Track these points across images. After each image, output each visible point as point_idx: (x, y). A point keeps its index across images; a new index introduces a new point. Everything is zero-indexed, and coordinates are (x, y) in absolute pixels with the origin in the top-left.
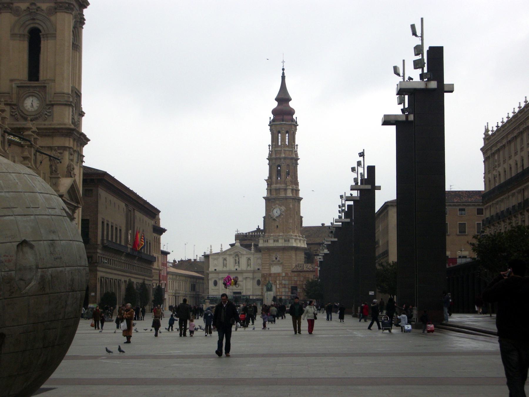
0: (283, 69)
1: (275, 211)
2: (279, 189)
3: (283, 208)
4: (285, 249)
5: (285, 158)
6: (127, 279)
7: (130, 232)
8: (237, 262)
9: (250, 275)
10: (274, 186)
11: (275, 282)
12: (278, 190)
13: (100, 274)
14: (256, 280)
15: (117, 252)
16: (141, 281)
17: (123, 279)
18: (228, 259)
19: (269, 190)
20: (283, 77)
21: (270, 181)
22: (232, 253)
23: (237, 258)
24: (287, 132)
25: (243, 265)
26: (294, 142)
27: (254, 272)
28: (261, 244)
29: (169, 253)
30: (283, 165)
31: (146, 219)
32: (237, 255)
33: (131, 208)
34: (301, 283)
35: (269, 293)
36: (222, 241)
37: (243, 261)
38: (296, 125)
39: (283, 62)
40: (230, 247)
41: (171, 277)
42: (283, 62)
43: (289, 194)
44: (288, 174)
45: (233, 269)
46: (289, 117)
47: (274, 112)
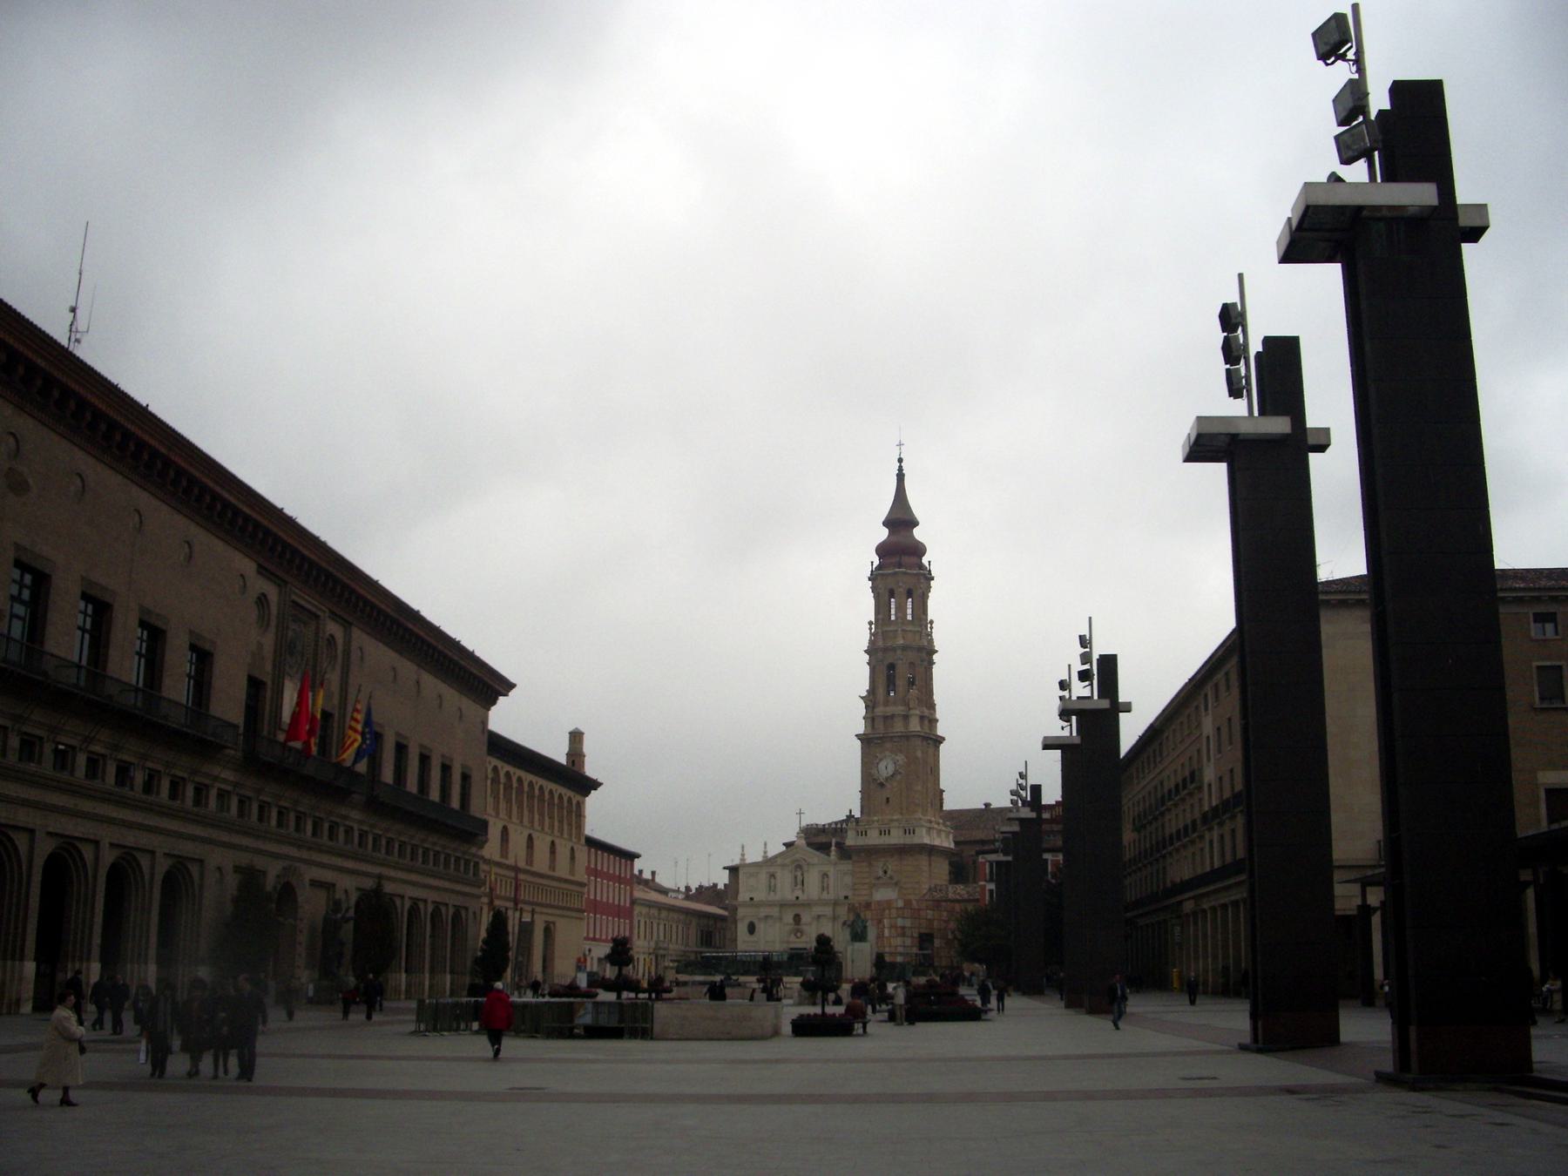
0: (900, 460)
1: (882, 765)
2: (893, 716)
3: (901, 758)
4: (903, 851)
5: (904, 648)
6: (244, 859)
8: (799, 878)
9: (828, 911)
10: (880, 710)
11: (880, 921)
12: (888, 719)
16: (369, 884)
17: (107, 835)
18: (778, 875)
19: (870, 718)
20: (901, 477)
21: (871, 700)
22: (787, 861)
24: (910, 594)
25: (813, 889)
26: (925, 612)
27: (836, 904)
28: (851, 840)
29: (638, 856)
30: (901, 662)
31: (469, 706)
32: (799, 867)
35: (857, 945)
36: (771, 835)
37: (813, 878)
38: (929, 577)
39: (900, 445)
41: (645, 910)
42: (900, 445)
43: (915, 726)
44: (912, 683)
45: (790, 897)
46: (914, 560)
47: (882, 550)
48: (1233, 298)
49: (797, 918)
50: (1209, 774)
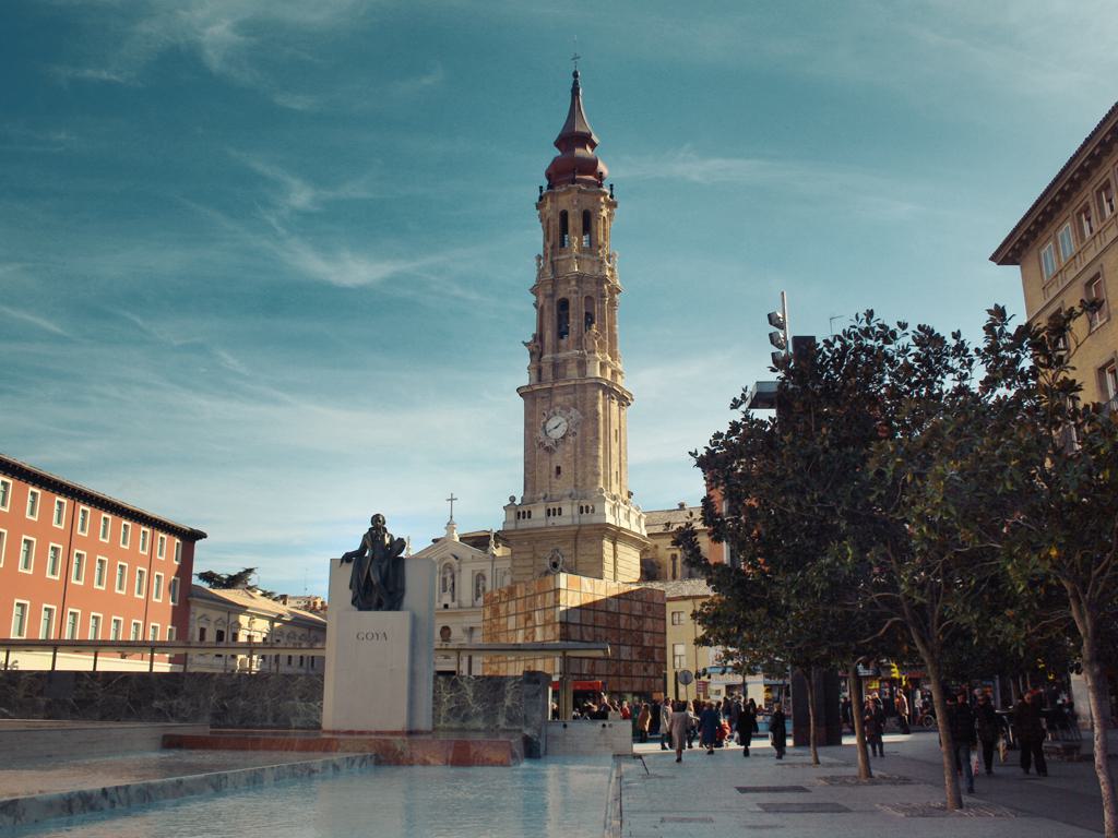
10: (547, 356)
11: (529, 617)
23: (449, 575)
34: (635, 624)
39: (576, 58)
42: (576, 58)
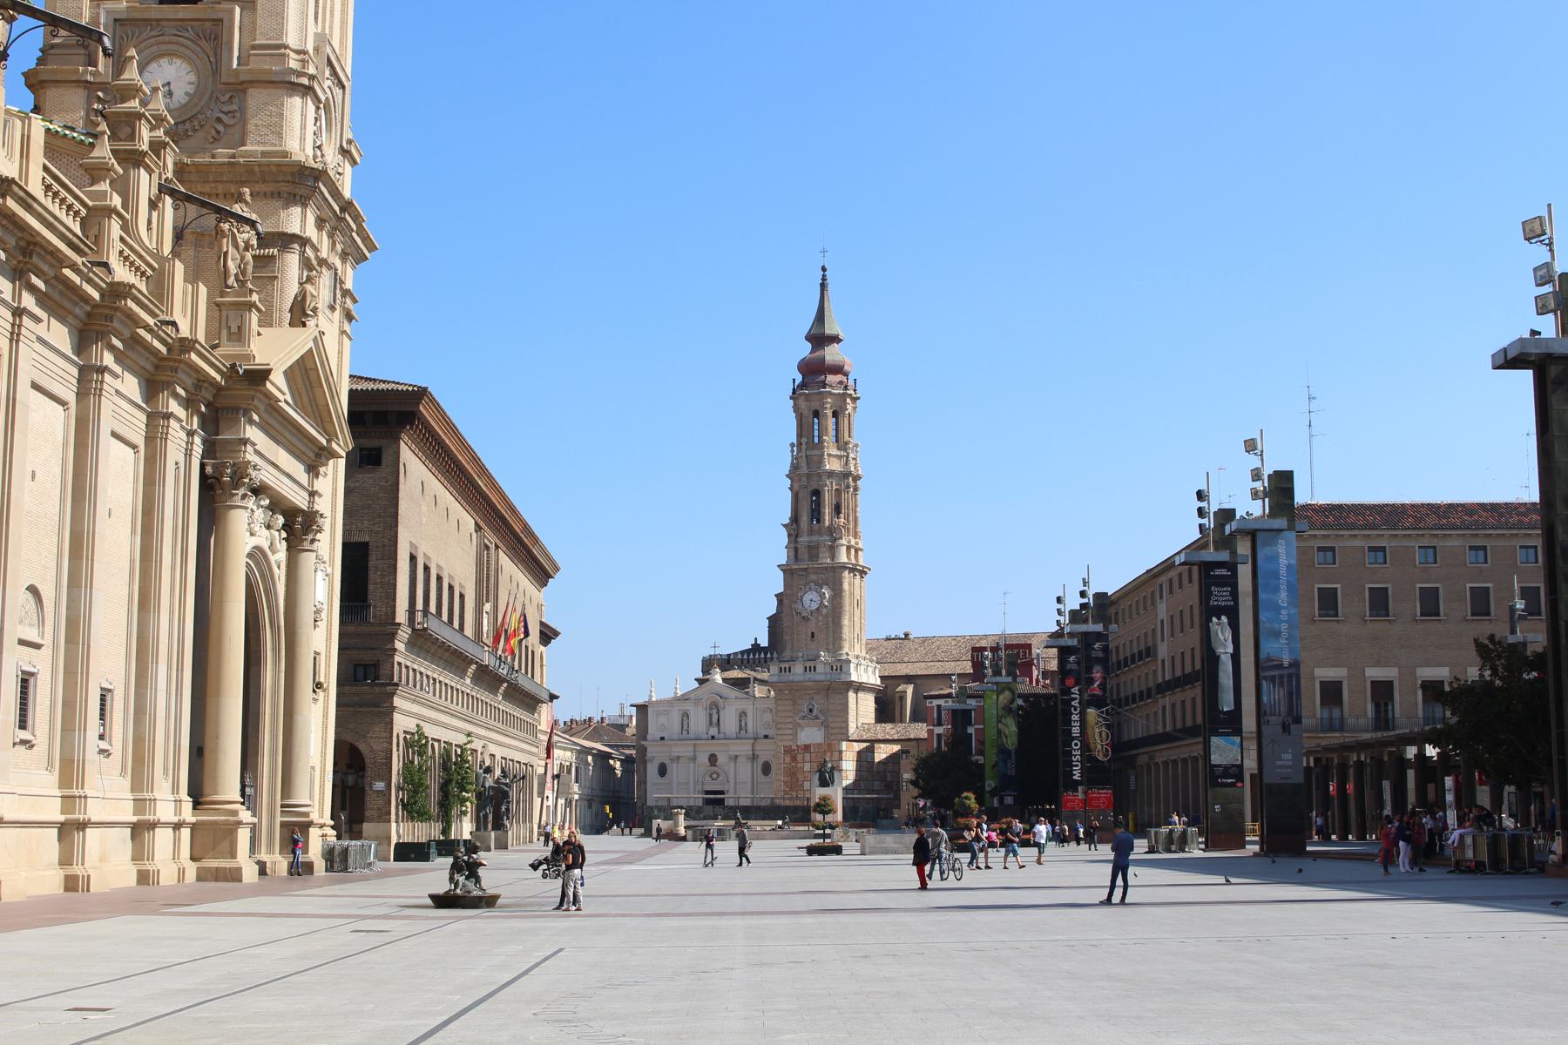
0: (824, 269)
1: (807, 598)
7: (487, 607)
10: (804, 539)
13: (402, 723)
14: (761, 761)
15: (455, 660)
20: (823, 286)
33: (491, 538)
39: (824, 251)
40: (696, 685)
42: (824, 251)
48: (1204, 487)
49: (713, 759)
50: (1163, 651)
